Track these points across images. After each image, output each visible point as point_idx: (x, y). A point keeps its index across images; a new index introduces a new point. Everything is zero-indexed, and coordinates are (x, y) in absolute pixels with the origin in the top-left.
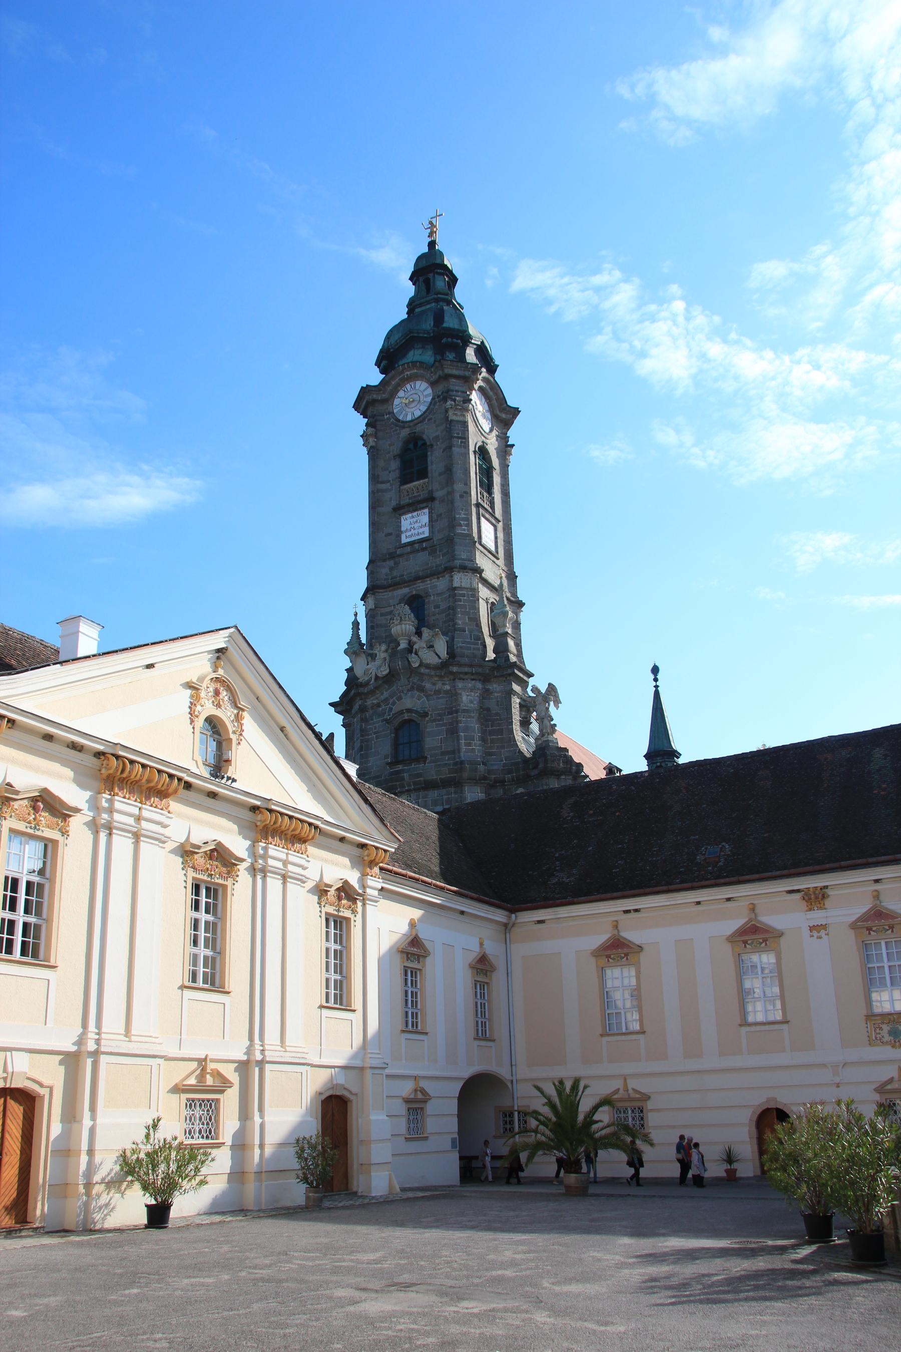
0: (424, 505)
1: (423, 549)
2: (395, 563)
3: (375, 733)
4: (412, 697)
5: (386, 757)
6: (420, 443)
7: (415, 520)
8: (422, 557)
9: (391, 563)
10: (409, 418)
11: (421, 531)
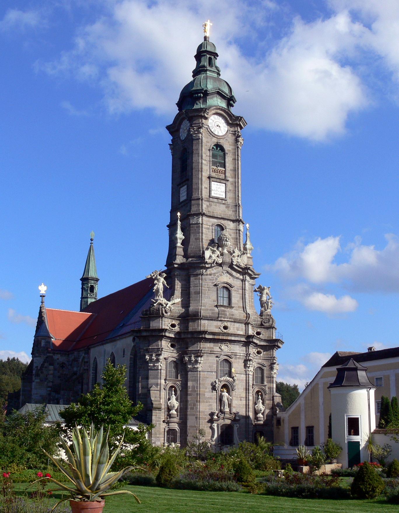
0: (224, 182)
1: (223, 204)
4: (227, 276)
5: (214, 301)
7: (219, 187)
8: (223, 207)
9: (208, 203)
11: (221, 193)
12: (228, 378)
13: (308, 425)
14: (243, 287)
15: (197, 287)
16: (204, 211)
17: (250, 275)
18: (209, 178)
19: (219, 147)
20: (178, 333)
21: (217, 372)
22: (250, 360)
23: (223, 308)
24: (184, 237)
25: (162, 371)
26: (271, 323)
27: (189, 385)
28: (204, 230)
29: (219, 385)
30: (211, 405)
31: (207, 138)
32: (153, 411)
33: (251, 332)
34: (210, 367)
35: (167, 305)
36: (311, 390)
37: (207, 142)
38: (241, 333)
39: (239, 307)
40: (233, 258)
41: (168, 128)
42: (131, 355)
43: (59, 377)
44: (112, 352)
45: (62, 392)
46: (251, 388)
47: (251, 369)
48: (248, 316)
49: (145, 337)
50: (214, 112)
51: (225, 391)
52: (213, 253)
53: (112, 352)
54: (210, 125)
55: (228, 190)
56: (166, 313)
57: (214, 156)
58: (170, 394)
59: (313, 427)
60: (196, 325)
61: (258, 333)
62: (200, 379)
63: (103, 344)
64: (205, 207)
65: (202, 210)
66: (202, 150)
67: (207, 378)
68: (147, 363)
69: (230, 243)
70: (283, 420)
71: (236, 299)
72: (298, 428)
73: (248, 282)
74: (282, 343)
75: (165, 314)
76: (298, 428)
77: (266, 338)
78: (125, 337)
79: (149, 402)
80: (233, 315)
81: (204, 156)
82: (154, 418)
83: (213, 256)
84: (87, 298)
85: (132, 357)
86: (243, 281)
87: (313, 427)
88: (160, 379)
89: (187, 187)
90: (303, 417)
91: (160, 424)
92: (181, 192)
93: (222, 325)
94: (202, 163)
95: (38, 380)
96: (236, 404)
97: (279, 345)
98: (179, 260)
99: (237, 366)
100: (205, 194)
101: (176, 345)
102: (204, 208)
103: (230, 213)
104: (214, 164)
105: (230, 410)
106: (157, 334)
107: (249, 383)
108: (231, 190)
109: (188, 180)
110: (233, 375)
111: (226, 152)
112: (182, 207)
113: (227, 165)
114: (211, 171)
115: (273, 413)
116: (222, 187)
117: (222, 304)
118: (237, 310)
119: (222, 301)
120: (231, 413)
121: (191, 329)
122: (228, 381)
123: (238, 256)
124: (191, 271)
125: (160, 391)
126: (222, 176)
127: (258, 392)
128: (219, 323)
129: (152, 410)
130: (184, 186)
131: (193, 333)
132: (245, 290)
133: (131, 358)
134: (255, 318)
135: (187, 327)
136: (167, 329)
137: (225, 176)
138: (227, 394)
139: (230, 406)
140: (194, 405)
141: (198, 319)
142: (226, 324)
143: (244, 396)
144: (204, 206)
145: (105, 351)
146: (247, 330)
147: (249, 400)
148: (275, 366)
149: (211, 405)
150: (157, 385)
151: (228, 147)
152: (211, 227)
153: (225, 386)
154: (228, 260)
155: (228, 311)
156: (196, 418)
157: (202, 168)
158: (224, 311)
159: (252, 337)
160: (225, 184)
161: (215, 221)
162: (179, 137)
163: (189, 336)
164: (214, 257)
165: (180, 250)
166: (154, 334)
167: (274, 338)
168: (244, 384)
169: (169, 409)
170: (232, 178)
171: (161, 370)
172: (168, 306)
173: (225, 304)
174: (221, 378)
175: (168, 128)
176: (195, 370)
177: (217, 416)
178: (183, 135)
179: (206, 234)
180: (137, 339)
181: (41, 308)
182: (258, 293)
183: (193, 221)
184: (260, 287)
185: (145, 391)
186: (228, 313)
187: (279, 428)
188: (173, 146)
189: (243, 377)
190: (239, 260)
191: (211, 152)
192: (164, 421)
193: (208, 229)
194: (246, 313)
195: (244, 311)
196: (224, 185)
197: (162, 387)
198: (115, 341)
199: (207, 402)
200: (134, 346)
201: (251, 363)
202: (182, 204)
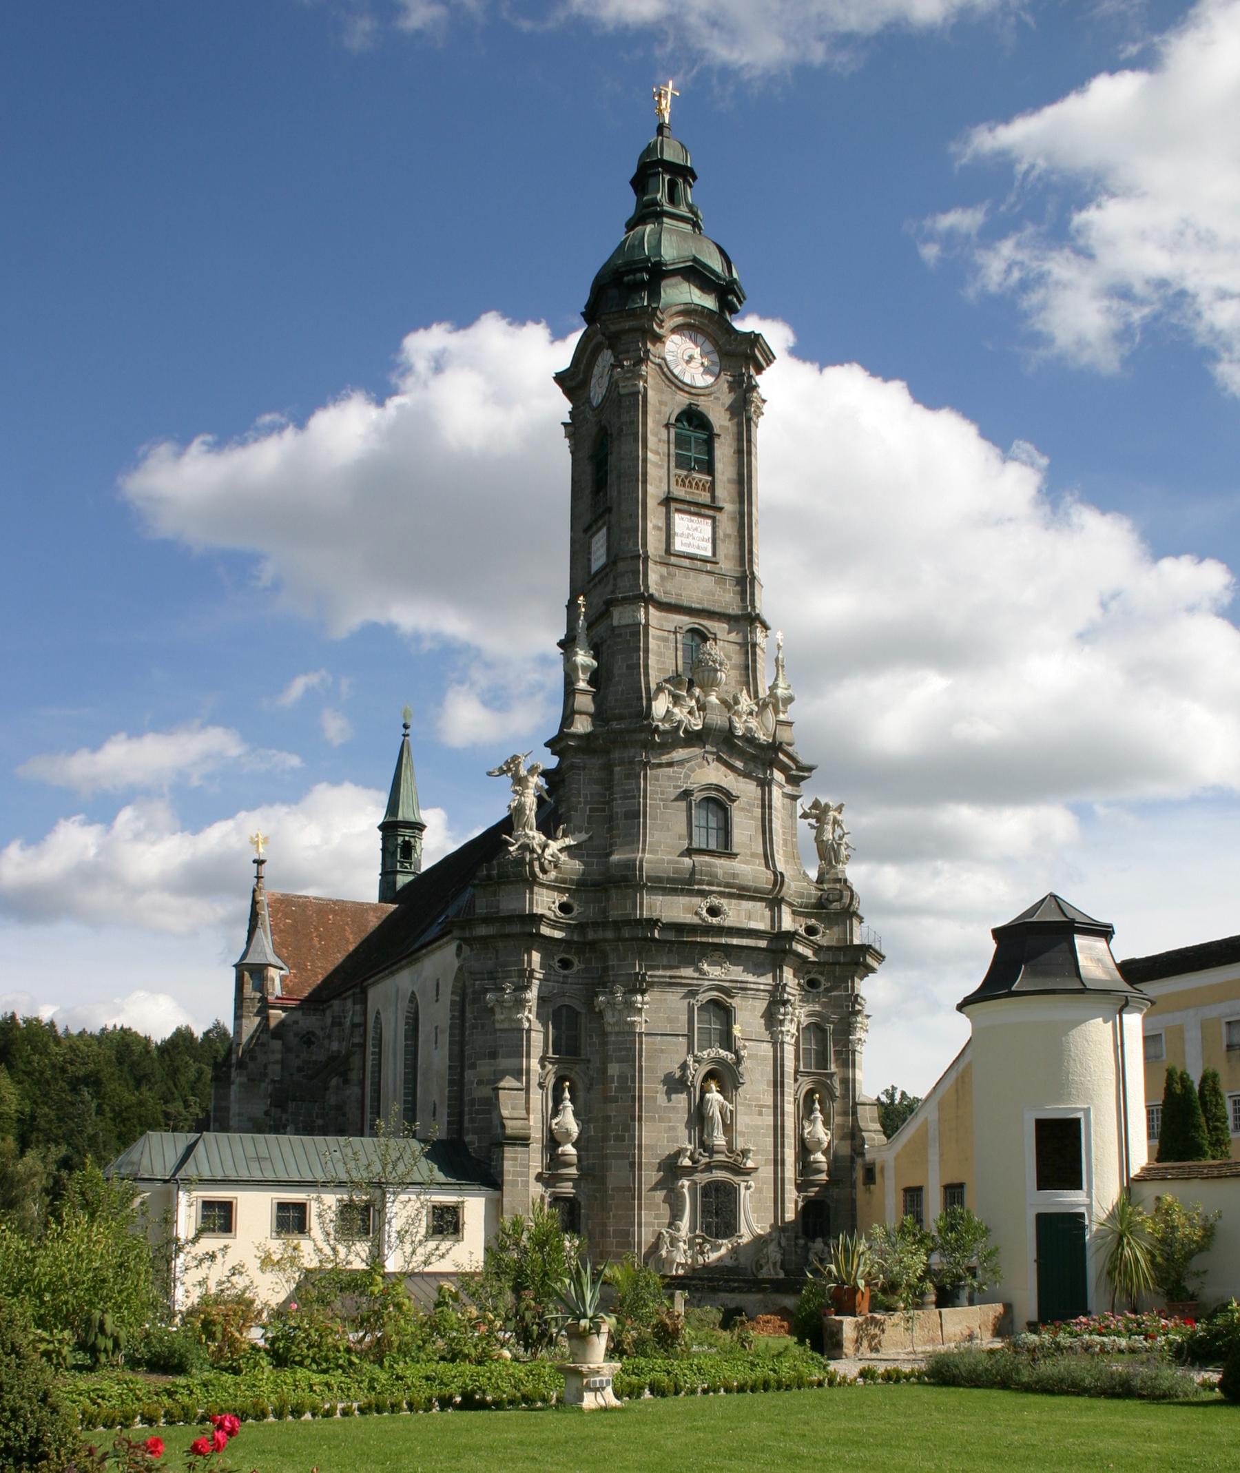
0: (710, 513)
1: (708, 572)
2: (669, 574)
3: (662, 800)
4: (718, 770)
6: (695, 422)
7: (695, 525)
8: (707, 582)
9: (664, 570)
10: (687, 380)
12: (723, 1053)
13: (948, 1181)
14: (763, 800)
15: (634, 797)
16: (651, 591)
17: (784, 769)
18: (668, 501)
19: (693, 418)
20: (581, 927)
21: (690, 1037)
22: (785, 1003)
23: (707, 858)
24: (595, 664)
25: (533, 1034)
26: (846, 900)
27: (610, 1072)
28: (652, 643)
29: (696, 1073)
30: (673, 1128)
31: (662, 392)
32: (506, 1149)
33: (788, 923)
34: (670, 1020)
35: (545, 847)
36: (957, 1080)
37: (661, 403)
38: (762, 925)
39: (753, 855)
40: (735, 719)
41: (560, 378)
42: (453, 993)
43: (300, 1069)
44: (413, 993)
45: (291, 1106)
46: (789, 1081)
47: (790, 1027)
48: (779, 879)
49: (483, 939)
50: (679, 320)
51: (713, 1086)
52: (675, 704)
53: (413, 993)
54: (669, 358)
55: (720, 533)
56: (544, 871)
57: (681, 442)
58: (558, 1100)
59: (961, 1186)
60: (629, 903)
61: (811, 931)
62: (640, 1056)
63: (392, 973)
64: (654, 579)
65: (647, 587)
66: (645, 424)
67: (662, 1051)
68: (492, 1010)
69: (727, 676)
70: (882, 1169)
71: (744, 829)
72: (920, 1189)
73: (781, 786)
74: (880, 957)
75: (541, 875)
76: (920, 1189)
77: (834, 944)
78: (440, 947)
79: (496, 1122)
80: (734, 875)
81: (652, 441)
82: (507, 1165)
83: (676, 710)
84: (397, 872)
85: (457, 999)
86: (765, 784)
87: (961, 1186)
88: (528, 1056)
89: (609, 530)
90: (933, 1155)
91: (526, 1184)
92: (593, 548)
93: (703, 904)
94: (645, 460)
95: (244, 1079)
96: (747, 1126)
97: (870, 960)
98: (582, 725)
99: (748, 1017)
100: (654, 544)
101: (576, 961)
102: (650, 583)
103: (727, 599)
104: (682, 462)
105: (730, 1143)
106: (516, 929)
107: (782, 1066)
108: (729, 536)
109: (609, 510)
110: (739, 1043)
111: (716, 431)
112: (595, 585)
113: (719, 466)
114: (673, 480)
115: (853, 1150)
116: (705, 527)
117: (704, 846)
118: (746, 863)
119: (704, 840)
120: (731, 1151)
121: (614, 914)
122: (720, 1061)
123: (751, 713)
124: (616, 755)
125: (527, 1090)
126: (705, 497)
127: (810, 1093)
128: (696, 900)
129: (502, 1145)
130: (599, 529)
131: (618, 925)
132: (770, 807)
133: (453, 1003)
134: (803, 887)
135: (604, 911)
136: (542, 916)
137: (713, 498)
138: (720, 1097)
139: (728, 1129)
140: (628, 1128)
141: (627, 887)
142: (715, 901)
143: (770, 1103)
144: (653, 578)
145: (397, 992)
146: (775, 919)
147: (783, 1114)
148: (859, 1019)
149: (673, 1128)
150: (517, 1073)
151: (719, 418)
152: (672, 636)
153: (710, 1075)
154: (718, 719)
155: (721, 866)
156: (632, 1164)
157: (645, 474)
158: (710, 865)
159: (791, 936)
160: (713, 519)
161: (685, 621)
162: (589, 401)
163: (609, 934)
164: (680, 713)
165: (584, 702)
166: (509, 929)
167: (856, 942)
168: (770, 1069)
169: (553, 1142)
170: (733, 503)
171: (529, 1031)
172: (548, 852)
173: (713, 846)
174: (701, 1049)
175: (560, 378)
176: (629, 1032)
177: (691, 1158)
178: (597, 392)
179: (660, 654)
180: (466, 949)
181: (254, 891)
182: (813, 821)
183: (619, 616)
184: (816, 805)
185: (486, 1091)
186: (720, 872)
187: (869, 1191)
188: (573, 429)
189: (766, 1049)
190: (753, 723)
191: (673, 431)
192: (539, 1178)
193: (665, 640)
194: (775, 873)
195: (767, 867)
196: (709, 521)
197: (534, 1080)
198: (417, 960)
199: (661, 1120)
200: (460, 968)
201: (790, 1009)
202: (597, 580)
